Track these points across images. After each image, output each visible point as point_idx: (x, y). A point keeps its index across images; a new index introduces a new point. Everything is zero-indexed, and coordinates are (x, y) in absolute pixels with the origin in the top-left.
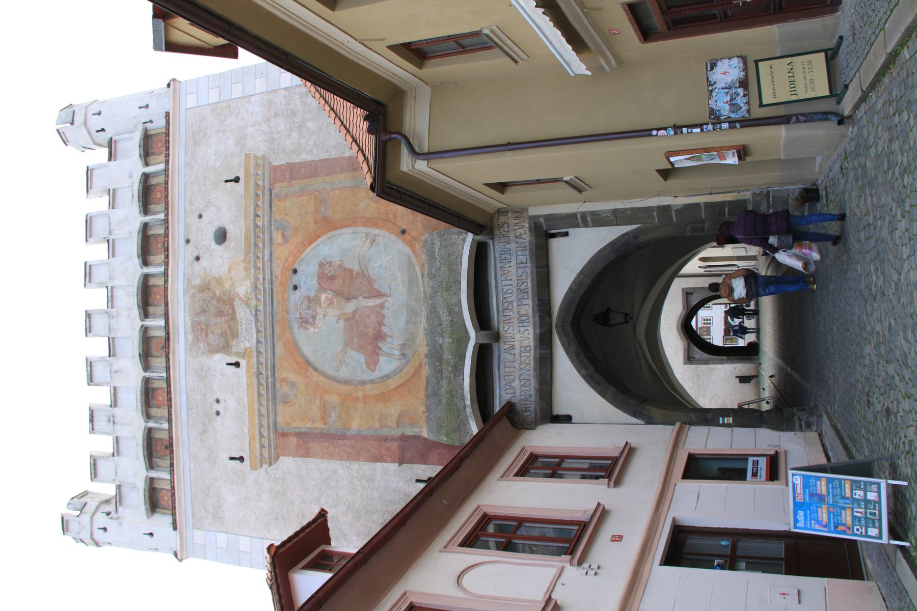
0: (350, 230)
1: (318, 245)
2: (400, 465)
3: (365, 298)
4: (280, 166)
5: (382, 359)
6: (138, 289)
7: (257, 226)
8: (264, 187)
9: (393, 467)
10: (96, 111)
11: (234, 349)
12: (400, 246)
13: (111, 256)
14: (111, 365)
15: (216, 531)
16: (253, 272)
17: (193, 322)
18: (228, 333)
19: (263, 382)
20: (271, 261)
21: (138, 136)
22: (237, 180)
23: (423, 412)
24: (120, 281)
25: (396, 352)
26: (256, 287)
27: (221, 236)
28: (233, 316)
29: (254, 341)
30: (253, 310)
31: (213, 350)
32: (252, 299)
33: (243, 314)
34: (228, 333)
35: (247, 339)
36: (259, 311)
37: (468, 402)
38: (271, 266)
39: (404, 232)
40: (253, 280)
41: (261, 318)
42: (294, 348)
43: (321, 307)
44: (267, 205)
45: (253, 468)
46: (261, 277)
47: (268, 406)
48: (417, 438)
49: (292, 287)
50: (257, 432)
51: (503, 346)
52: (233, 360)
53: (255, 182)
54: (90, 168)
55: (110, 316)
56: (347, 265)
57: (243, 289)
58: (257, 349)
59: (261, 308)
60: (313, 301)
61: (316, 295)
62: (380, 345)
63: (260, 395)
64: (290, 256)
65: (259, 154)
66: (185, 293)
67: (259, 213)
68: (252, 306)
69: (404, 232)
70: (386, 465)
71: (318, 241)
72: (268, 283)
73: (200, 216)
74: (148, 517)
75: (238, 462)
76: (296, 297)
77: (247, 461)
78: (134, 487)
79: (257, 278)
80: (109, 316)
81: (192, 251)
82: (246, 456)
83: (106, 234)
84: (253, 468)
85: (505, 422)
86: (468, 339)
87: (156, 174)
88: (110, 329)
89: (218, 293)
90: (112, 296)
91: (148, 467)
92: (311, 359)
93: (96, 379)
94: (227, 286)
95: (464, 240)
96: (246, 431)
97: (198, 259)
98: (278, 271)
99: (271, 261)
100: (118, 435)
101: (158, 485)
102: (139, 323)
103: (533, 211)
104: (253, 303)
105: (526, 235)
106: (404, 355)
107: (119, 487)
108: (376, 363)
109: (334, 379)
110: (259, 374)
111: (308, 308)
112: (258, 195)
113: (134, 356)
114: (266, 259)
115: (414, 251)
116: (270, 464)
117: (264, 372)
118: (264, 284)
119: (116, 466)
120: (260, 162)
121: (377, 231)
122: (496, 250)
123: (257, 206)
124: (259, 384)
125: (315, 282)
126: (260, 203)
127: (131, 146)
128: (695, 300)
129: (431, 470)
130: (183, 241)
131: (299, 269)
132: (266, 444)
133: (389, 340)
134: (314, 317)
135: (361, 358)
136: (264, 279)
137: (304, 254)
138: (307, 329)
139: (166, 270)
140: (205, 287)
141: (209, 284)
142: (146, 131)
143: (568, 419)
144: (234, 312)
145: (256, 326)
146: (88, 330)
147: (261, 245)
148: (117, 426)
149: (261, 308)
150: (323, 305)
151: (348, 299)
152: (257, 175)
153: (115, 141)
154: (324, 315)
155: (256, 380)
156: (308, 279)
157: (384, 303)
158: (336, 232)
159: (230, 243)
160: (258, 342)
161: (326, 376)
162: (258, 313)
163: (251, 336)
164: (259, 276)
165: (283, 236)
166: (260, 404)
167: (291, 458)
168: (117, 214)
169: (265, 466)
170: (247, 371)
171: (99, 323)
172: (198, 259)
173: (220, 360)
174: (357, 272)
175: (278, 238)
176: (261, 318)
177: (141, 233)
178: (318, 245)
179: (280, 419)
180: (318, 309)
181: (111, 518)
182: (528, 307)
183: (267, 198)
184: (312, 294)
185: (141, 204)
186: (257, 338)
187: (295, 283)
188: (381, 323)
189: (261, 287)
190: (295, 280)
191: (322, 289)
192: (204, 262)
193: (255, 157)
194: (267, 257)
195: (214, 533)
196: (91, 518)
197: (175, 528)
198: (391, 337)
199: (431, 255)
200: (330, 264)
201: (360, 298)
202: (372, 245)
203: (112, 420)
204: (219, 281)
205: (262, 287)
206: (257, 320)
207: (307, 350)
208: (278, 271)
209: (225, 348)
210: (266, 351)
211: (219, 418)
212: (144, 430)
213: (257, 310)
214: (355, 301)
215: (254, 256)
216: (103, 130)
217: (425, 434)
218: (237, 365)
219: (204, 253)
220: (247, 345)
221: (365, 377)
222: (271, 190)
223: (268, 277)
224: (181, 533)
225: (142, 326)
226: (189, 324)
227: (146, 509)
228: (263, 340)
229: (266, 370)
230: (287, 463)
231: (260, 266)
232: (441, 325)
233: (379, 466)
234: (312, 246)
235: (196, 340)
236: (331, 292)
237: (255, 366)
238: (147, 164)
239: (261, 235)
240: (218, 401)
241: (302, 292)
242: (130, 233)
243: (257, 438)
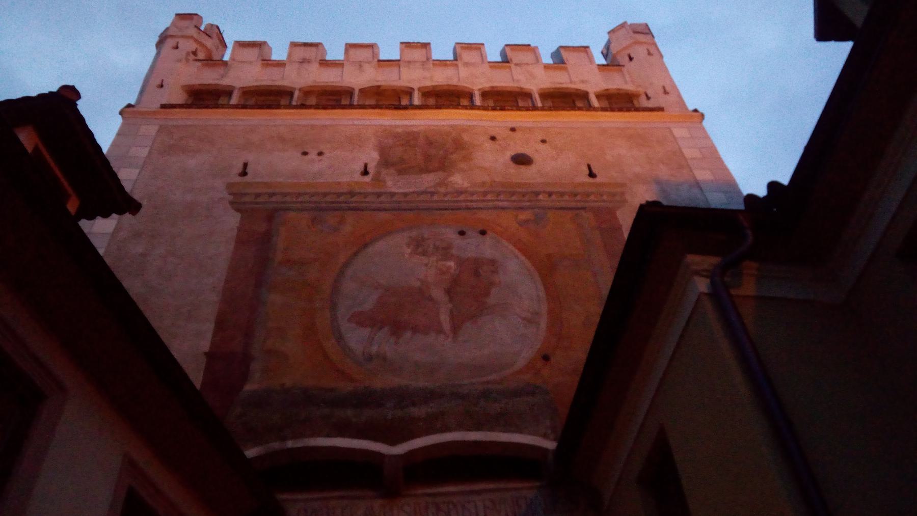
0: (542, 294)
1: (518, 258)
2: (206, 354)
3: (451, 312)
4: (616, 218)
5: (365, 332)
6: (457, 86)
7: (537, 194)
8: (587, 202)
9: (205, 345)
10: (651, 52)
11: (384, 172)
12: (526, 355)
13: (491, 64)
14: (369, 62)
15: (152, 147)
16: (480, 190)
17: (415, 132)
18: (404, 166)
19: (342, 198)
20: (495, 208)
21: (630, 87)
22: (592, 175)
23: (283, 385)
24: (463, 72)
25: (374, 349)
26: (460, 192)
27: (521, 160)
28: (425, 170)
29: (394, 190)
30: (432, 190)
31: (383, 151)
32: (447, 188)
33: (428, 180)
34: (404, 166)
35: (394, 184)
36: (431, 196)
37: (290, 444)
38: (489, 209)
39: (546, 358)
40: (471, 190)
41: (422, 198)
42: (385, 231)
43: (437, 261)
44: (563, 204)
45: (230, 186)
46: (475, 198)
47: (310, 202)
48: (245, 377)
49: (464, 229)
50: (277, 190)
52: (371, 169)
53: (593, 193)
54: (587, 49)
55: (423, 63)
56: (494, 291)
57: (458, 180)
58: (385, 193)
59: (436, 197)
60: (445, 252)
61: (452, 255)
62: (386, 329)
63: (325, 195)
64: (501, 227)
65: (628, 197)
66: (451, 126)
67: (554, 197)
68: (438, 188)
69: (546, 358)
70: (209, 336)
71: (523, 258)
72: (466, 205)
73: (543, 141)
74: (183, 87)
75: (240, 170)
76: (450, 234)
77: (239, 179)
78: (223, 76)
79: (472, 194)
80: (424, 62)
82: (247, 179)
83: (515, 61)
84: (230, 186)
86: (393, 443)
88: (409, 62)
89: (454, 156)
90: (446, 65)
91: (245, 90)
92: (370, 250)
93: (352, 52)
94: (462, 165)
95: (545, 436)
96: (281, 180)
97: (493, 138)
98: (482, 215)
99: (495, 208)
100: (287, 65)
102: (416, 86)
104: (442, 190)
106: (370, 358)
107: (225, 64)
108: (361, 324)
109: (341, 273)
110: (352, 194)
111: (436, 248)
112: (576, 195)
113: (377, 81)
114: (497, 203)
115: (520, 372)
116: (231, 203)
117: (353, 199)
118: (465, 201)
119: (251, 63)
120: (618, 198)
121: (543, 324)
123: (562, 194)
124: (339, 195)
126: (566, 197)
127: (616, 82)
130: (514, 125)
131: (488, 239)
132: (260, 200)
133: (392, 340)
134: (424, 253)
135: (368, 305)
136: (472, 201)
137: (506, 243)
138: (408, 245)
139: (479, 108)
140: (459, 145)
141: (463, 149)
144: (428, 171)
145: (413, 193)
146: (408, 45)
147: (514, 198)
148: (297, 65)
149: (436, 197)
150: (441, 263)
151: (448, 292)
152: (602, 195)
153: (621, 71)
154: (426, 265)
155: (345, 191)
157: (445, 334)
158: (537, 278)
159: (514, 169)
160: (393, 194)
161: (347, 264)
162: (429, 195)
163: (400, 187)
164: (475, 195)
165: (527, 221)
166: (312, 195)
167: (237, 225)
168: (539, 72)
169: (231, 198)
170: (356, 183)
171: (418, 55)
172: (493, 138)
173: (372, 157)
174: (486, 302)
175: (523, 216)
176: (422, 198)
177: (518, 90)
178: (518, 258)
179: (292, 214)
180: (434, 258)
181: (188, 54)
183: (573, 204)
184: (454, 251)
185: (552, 90)
186: (397, 193)
187: (469, 233)
188: (415, 330)
189: (462, 198)
191: (461, 262)
192: (488, 145)
193: (623, 194)
194: (500, 204)
195: (150, 144)
196: (192, 37)
197: (163, 106)
198: (396, 343)
199: (516, 393)
200: (495, 272)
201: (450, 306)
202: (524, 319)
203: (304, 61)
204: (467, 158)
205: (462, 199)
206: (419, 194)
207: (380, 246)
208: (482, 215)
209: (386, 162)
210: (381, 202)
211: (299, 155)
212: (293, 88)
213: (432, 194)
214: (446, 299)
215: (500, 192)
216: (631, 59)
217: (248, 387)
218: (365, 172)
219: (500, 145)
220: (389, 183)
222: (584, 208)
223: (474, 205)
224: (154, 113)
225: (413, 89)
226: (415, 130)
227: (194, 85)
228: (395, 199)
229: (355, 202)
230: (233, 220)
231: (489, 197)
232: (414, 405)
233: (210, 327)
234: (516, 251)
235: (396, 136)
236: (457, 272)
237: (362, 191)
238: (599, 96)
239: (526, 198)
240: (320, 154)
241: (458, 241)
242: (518, 81)
243: (270, 191)
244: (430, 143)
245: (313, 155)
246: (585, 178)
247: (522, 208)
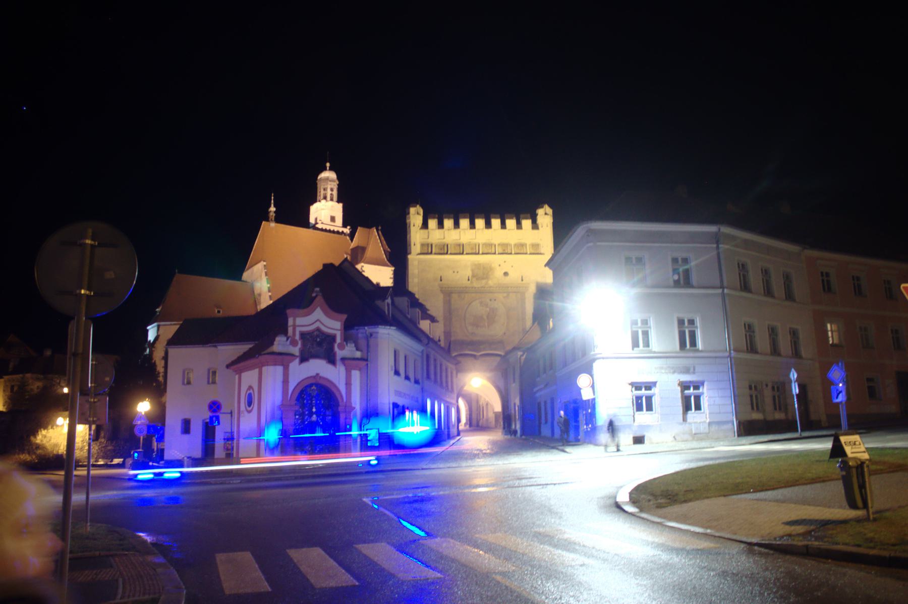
7: (508, 287)
9: (443, 330)
22: (522, 280)
26: (491, 287)
27: (506, 274)
31: (473, 270)
77: (441, 282)
87: (526, 248)
122: (498, 359)
160: (475, 288)
206: (482, 287)
207: (474, 303)
209: (473, 276)
213: (484, 287)
218: (469, 280)
230: (441, 296)
244: (484, 268)
246: (520, 281)
247: (504, 292)
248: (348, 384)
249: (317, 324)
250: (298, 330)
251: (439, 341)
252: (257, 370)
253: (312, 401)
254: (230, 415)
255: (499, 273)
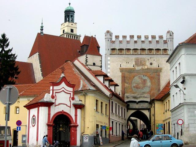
22: (159, 67)
31: (135, 62)
35: (137, 68)
51: (136, 104)
65: (162, 71)
76: (142, 76)
81: (149, 58)
84: (120, 68)
85: (127, 105)
92: (134, 78)
101: (115, 50)
103: (151, 108)
105: (149, 108)
122: (146, 104)
125: (144, 79)
128: (135, 122)
129: (121, 96)
142: (167, 49)
143: (127, 111)
156: (146, 78)
173: (134, 63)
182: (140, 107)
190: (145, 76)
192: (147, 61)
207: (136, 77)
209: (136, 64)
218: (133, 66)
221: (132, 86)
240: (128, 63)
245: (128, 63)
246: (158, 67)
248: (76, 115)
249: (63, 89)
250: (54, 91)
251: (120, 94)
252: (37, 109)
253: (60, 122)
254: (25, 126)
255: (148, 64)
